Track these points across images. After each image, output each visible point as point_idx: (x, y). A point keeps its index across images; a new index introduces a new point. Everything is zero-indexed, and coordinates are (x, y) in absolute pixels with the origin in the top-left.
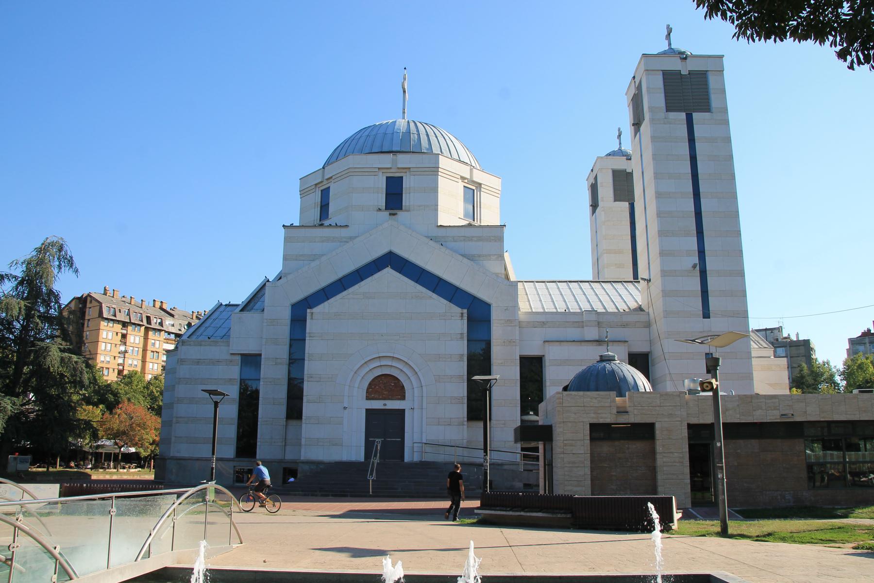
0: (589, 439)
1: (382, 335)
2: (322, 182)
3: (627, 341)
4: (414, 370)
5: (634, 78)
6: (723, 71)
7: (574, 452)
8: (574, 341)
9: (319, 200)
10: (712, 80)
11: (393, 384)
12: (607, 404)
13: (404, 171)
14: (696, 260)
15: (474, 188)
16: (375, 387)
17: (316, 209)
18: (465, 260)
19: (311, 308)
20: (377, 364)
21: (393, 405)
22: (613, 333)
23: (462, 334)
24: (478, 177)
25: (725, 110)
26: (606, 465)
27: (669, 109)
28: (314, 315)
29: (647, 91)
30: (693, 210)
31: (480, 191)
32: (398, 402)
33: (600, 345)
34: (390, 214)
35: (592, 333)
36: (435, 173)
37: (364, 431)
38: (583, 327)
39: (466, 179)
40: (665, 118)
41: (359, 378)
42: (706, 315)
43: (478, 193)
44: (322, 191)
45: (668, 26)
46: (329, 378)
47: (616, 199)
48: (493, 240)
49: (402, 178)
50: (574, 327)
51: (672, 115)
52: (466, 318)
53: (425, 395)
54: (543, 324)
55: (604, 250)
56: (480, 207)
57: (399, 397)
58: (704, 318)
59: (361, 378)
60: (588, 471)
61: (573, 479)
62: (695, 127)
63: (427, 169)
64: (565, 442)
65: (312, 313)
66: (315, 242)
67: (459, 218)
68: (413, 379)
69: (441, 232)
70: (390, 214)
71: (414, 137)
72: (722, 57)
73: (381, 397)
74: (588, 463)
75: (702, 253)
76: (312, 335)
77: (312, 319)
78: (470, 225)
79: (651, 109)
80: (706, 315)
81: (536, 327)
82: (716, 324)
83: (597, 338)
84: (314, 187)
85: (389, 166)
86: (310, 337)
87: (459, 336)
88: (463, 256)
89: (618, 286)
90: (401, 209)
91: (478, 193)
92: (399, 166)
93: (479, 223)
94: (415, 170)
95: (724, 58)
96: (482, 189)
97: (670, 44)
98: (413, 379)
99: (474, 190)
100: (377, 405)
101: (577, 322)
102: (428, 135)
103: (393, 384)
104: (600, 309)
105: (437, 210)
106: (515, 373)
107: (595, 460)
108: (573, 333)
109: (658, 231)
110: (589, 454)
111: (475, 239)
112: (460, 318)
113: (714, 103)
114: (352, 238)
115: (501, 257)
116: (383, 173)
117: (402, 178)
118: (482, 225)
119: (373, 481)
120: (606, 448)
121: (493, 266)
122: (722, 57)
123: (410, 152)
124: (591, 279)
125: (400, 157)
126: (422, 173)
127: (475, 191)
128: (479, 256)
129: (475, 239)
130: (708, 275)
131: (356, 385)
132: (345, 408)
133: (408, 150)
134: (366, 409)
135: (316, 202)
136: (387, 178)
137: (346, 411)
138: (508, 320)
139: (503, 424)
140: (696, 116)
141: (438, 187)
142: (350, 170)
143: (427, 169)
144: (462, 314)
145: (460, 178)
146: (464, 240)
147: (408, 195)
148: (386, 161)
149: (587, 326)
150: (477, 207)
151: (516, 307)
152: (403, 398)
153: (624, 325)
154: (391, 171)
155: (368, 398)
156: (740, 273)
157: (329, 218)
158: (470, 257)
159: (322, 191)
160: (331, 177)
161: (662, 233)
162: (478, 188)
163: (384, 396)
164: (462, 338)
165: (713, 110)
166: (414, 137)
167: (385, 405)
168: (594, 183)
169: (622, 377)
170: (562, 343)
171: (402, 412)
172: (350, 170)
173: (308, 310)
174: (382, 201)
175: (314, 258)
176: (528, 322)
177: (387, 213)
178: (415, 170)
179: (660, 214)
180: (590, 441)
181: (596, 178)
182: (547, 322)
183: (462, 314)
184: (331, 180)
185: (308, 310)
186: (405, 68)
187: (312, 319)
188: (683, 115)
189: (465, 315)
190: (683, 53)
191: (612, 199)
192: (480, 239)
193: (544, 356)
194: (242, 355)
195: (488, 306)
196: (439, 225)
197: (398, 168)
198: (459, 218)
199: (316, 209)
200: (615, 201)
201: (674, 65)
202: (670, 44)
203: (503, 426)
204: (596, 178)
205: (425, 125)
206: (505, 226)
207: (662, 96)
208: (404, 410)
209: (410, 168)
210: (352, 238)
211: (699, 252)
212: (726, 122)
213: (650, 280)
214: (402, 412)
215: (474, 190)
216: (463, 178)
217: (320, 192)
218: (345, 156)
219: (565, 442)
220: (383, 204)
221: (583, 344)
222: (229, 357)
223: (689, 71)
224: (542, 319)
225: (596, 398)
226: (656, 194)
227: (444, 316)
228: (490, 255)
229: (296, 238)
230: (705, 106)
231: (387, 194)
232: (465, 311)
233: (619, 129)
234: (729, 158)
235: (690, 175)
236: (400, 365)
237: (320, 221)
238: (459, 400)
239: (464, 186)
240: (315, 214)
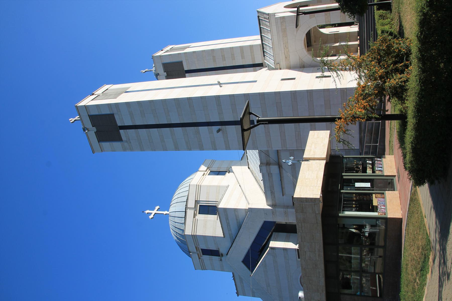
8: (281, 180)
15: (198, 205)
31: (200, 201)
38: (272, 174)
39: (194, 213)
43: (201, 202)
48: (226, 213)
54: (272, 193)
63: (194, 240)
91: (201, 202)
96: (198, 200)
101: (268, 174)
111: (228, 221)
121: (241, 215)
126: (197, 241)
128: (237, 220)
143: (194, 240)
150: (209, 204)
176: (272, 200)
195: (265, 223)
196: (223, 236)
197: (197, 251)
198: (217, 219)
224: (269, 193)
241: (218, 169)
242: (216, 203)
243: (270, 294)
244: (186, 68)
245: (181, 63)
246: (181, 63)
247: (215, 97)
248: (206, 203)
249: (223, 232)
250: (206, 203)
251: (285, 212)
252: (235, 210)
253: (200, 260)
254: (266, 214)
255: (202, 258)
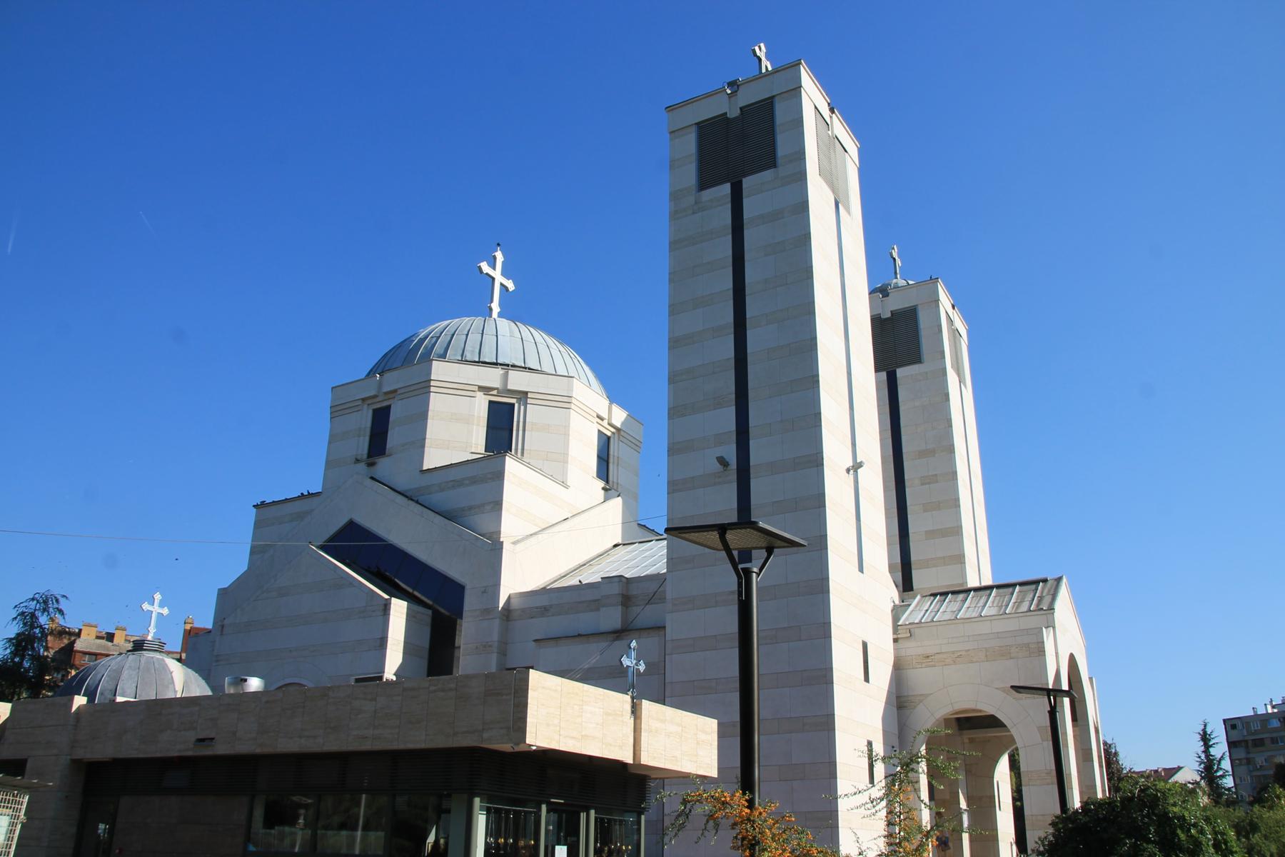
1: (291, 651)
8: (579, 635)
31: (526, 404)
36: (424, 390)
39: (493, 389)
43: (522, 408)
54: (544, 611)
85: (372, 393)
91: (522, 408)
94: (403, 391)
96: (529, 401)
111: (467, 482)
116: (369, 405)
121: (482, 521)
128: (470, 508)
129: (467, 482)
138: (485, 609)
154: (378, 400)
162: (523, 399)
176: (523, 610)
178: (403, 391)
182: (551, 606)
196: (424, 468)
197: (386, 393)
198: (472, 453)
224: (543, 601)
228: (483, 505)
241: (616, 458)
242: (519, 451)
244: (900, 372)
245: (916, 358)
246: (916, 358)
247: (818, 455)
248: (518, 422)
249: (436, 468)
250: (518, 422)
252: (497, 504)
253: (360, 403)
254: (484, 592)
255: (366, 406)
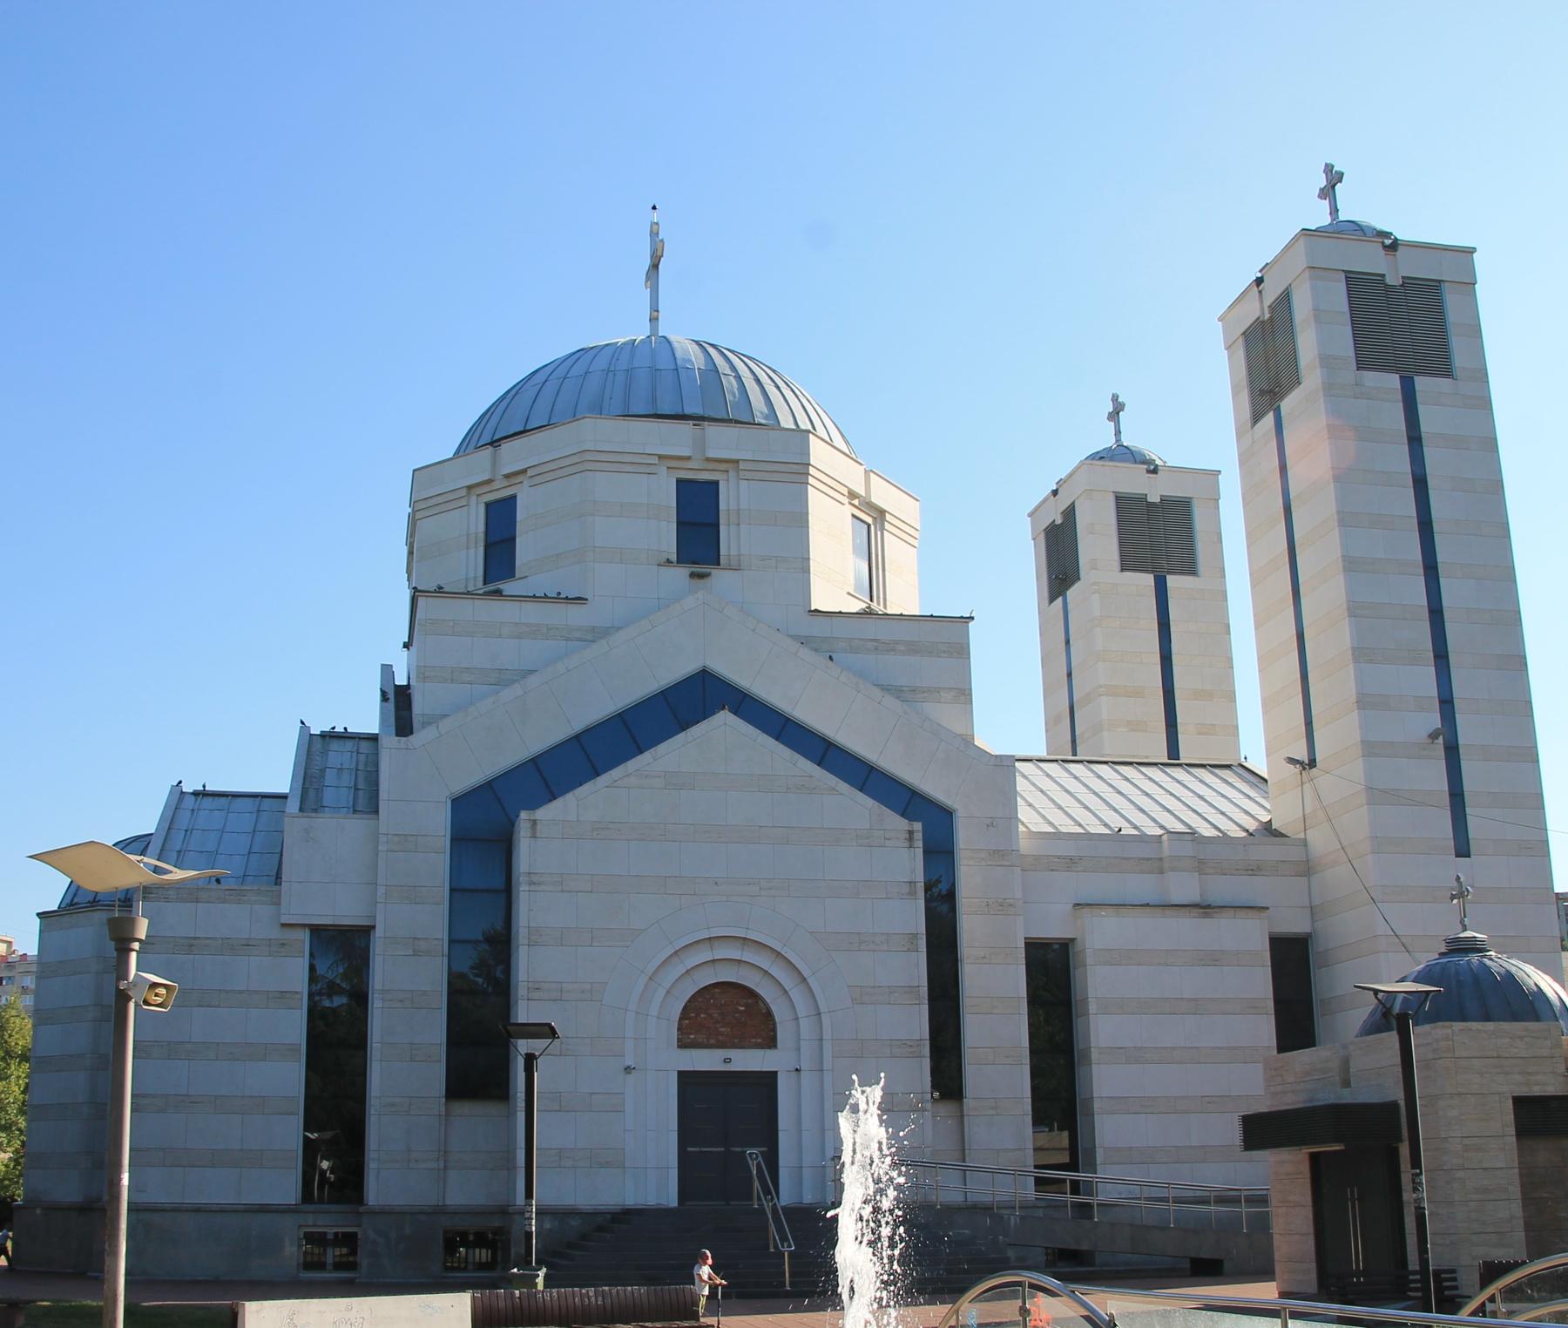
0: (1514, 1133)
1: (716, 883)
2: (490, 481)
3: (1268, 908)
4: (799, 972)
5: (1259, 281)
6: (1474, 284)
7: (1485, 1166)
8: (1148, 905)
9: (482, 528)
10: (1451, 301)
11: (742, 1008)
12: (1546, 1052)
13: (723, 466)
14: (1435, 721)
15: (869, 520)
16: (698, 1015)
17: (472, 551)
18: (889, 701)
19: (533, 805)
20: (705, 955)
21: (747, 1060)
22: (1223, 888)
23: (912, 883)
24: (883, 495)
25: (1481, 376)
26: (1546, 1195)
27: (1362, 364)
28: (538, 827)
29: (1315, 316)
30: (1425, 602)
31: (883, 529)
32: (759, 1053)
33: (1206, 915)
34: (692, 575)
35: (1185, 888)
37: (676, 1127)
40: (1357, 385)
41: (661, 992)
42: (1463, 850)
43: (879, 533)
44: (488, 505)
45: (1329, 169)
46: (583, 992)
47: (1127, 564)
48: (944, 652)
49: (715, 485)
50: (1142, 872)
51: (1371, 378)
52: (920, 844)
53: (827, 1035)
54: (1071, 863)
55: (1101, 687)
56: (884, 570)
57: (759, 1041)
58: (1457, 856)
59: (665, 991)
60: (1516, 1208)
61: (1488, 1230)
62: (1421, 408)
64: (1466, 1141)
65: (534, 822)
66: (500, 636)
67: (849, 594)
68: (797, 995)
69: (818, 628)
70: (692, 575)
71: (730, 383)
72: (1471, 251)
73: (712, 1041)
74: (1515, 1190)
75: (1446, 703)
76: (535, 879)
77: (534, 836)
78: (868, 613)
79: (1326, 361)
80: (1463, 850)
81: (1057, 870)
82: (1479, 870)
83: (1195, 897)
84: (463, 493)
86: (532, 883)
87: (906, 889)
88: (886, 689)
89: (1127, 771)
90: (717, 562)
91: (879, 533)
92: (711, 454)
93: (882, 608)
95: (1475, 255)
96: (887, 526)
97: (1334, 211)
98: (797, 995)
99: (869, 526)
100: (707, 1060)
101: (1148, 859)
102: (758, 381)
103: (742, 1008)
104: (1068, 827)
105: (807, 571)
106: (1015, 980)
107: (1531, 1182)
108: (1141, 886)
109: (1354, 649)
110: (1517, 1170)
112: (907, 844)
113: (1459, 360)
114: (597, 634)
115: (964, 694)
117: (716, 483)
118: (889, 612)
119: (790, 1253)
120: (1545, 1153)
122: (1471, 251)
123: (730, 421)
124: (1043, 754)
125: (712, 430)
127: (872, 527)
129: (902, 648)
130: (1461, 757)
131: (654, 1011)
132: (628, 1069)
133: (723, 416)
134: (679, 1072)
135: (473, 530)
136: (680, 482)
137: (631, 1078)
139: (992, 1108)
140: (1421, 383)
141: (808, 513)
142: (588, 457)
144: (911, 833)
145: (847, 494)
146: (876, 649)
147: (733, 528)
148: (676, 439)
149: (1173, 869)
151: (1013, 818)
152: (771, 1042)
153: (1254, 870)
154: (690, 465)
155: (682, 1045)
156: (1530, 756)
157: (517, 575)
158: (897, 692)
159: (488, 505)
160: (524, 471)
161: (1363, 654)
162: (878, 520)
163: (721, 1038)
164: (912, 893)
165: (1458, 373)
166: (731, 384)
167: (727, 1061)
168: (1059, 521)
169: (1535, 989)
170: (1123, 910)
171: (769, 1079)
172: (588, 457)
173: (524, 815)
174: (666, 537)
175: (503, 679)
176: (1037, 858)
177: (683, 572)
179: (1355, 610)
180: (1517, 1139)
181: (1070, 513)
182: (1081, 858)
183: (911, 833)
184: (520, 478)
185: (524, 815)
186: (654, 208)
187: (534, 836)
188: (1394, 381)
189: (919, 836)
190: (1387, 235)
191: (1116, 564)
192: (913, 648)
193: (1073, 940)
194: (316, 931)
196: (813, 609)
197: (708, 460)
198: (849, 594)
199: (472, 551)
200: (1122, 570)
201: (1371, 261)
202: (1334, 211)
203: (993, 1112)
204: (1070, 513)
205: (711, 350)
206: (972, 618)
207: (1347, 330)
208: (776, 1072)
209: (737, 461)
210: (597, 634)
211: (1442, 702)
212: (1485, 403)
213: (1312, 763)
214: (769, 1079)
215: (869, 526)
216: (852, 495)
217: (483, 505)
218: (574, 417)
219: (1466, 1141)
220: (670, 546)
221: (1168, 912)
222: (276, 933)
223: (1403, 277)
224: (1069, 850)
225: (1521, 1038)
226: (1343, 561)
227: (867, 838)
228: (938, 690)
229: (451, 624)
230: (1442, 366)
231: (678, 524)
232: (918, 826)
233: (1115, 398)
234: (1495, 487)
235: (1415, 521)
236: (763, 961)
237: (485, 584)
238: (911, 1050)
239: (854, 516)
240: (469, 563)
242: (882, 600)
243: (616, 784)
244: (1173, 581)
245: (1190, 568)
246: (1190, 568)
249: (840, 612)
251: (1011, 905)
252: (963, 694)
